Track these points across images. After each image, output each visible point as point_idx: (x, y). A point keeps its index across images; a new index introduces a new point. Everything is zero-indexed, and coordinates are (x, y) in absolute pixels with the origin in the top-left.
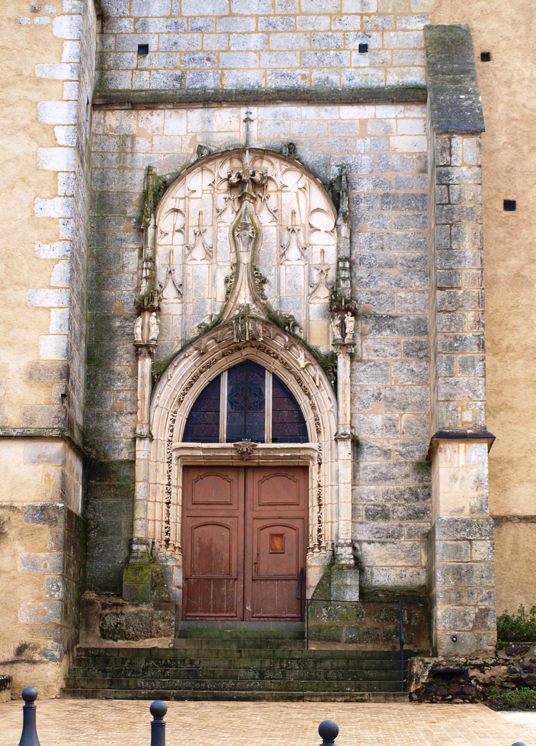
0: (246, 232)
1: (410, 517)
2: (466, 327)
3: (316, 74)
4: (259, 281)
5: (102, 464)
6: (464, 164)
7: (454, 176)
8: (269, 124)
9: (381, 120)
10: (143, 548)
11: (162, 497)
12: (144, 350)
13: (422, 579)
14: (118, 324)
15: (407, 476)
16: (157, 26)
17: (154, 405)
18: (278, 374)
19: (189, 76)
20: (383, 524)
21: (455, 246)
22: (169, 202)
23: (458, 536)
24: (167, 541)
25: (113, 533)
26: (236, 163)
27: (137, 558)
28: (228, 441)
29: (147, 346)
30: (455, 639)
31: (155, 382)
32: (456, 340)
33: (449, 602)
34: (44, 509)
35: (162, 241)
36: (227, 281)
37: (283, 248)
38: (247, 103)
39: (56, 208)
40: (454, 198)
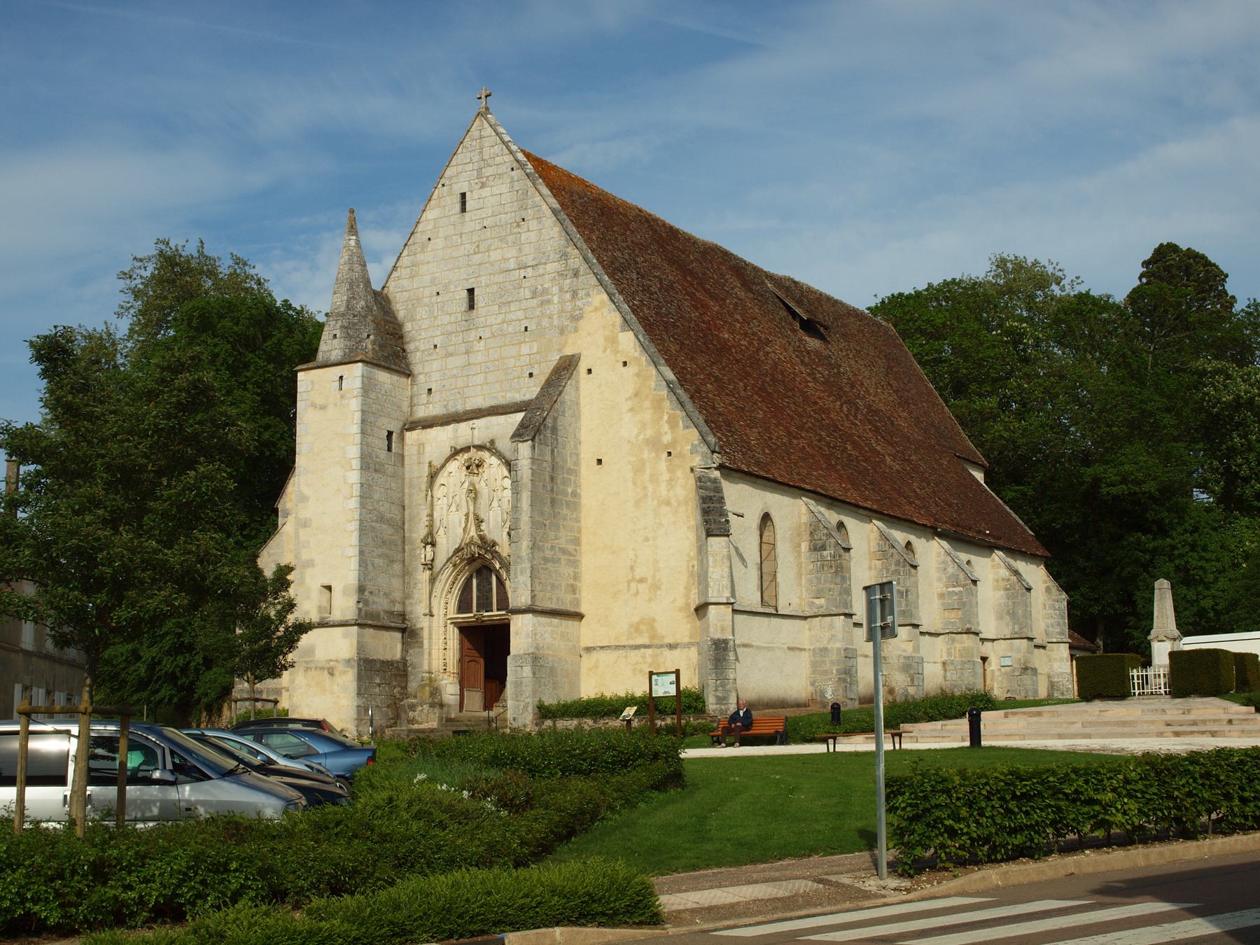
0: (473, 493)
3: (509, 395)
4: (479, 521)
16: (435, 376)
19: (450, 404)
22: (440, 479)
34: (349, 660)
39: (354, 503)
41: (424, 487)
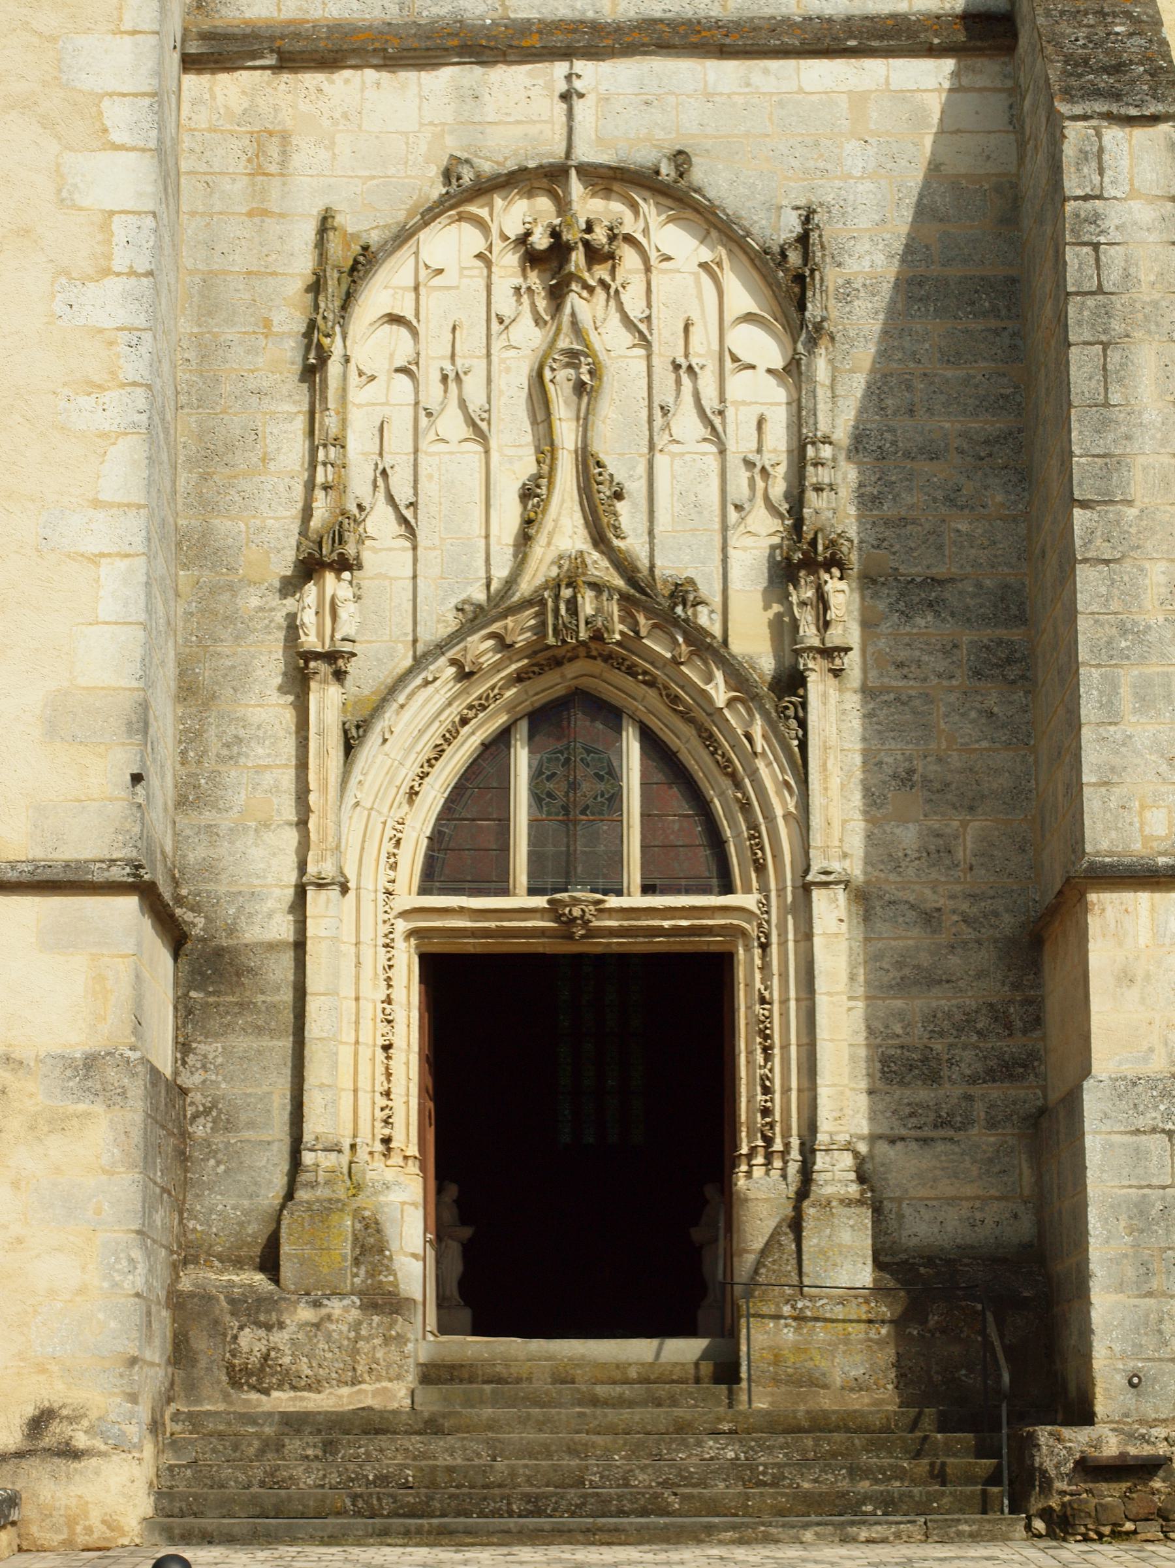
1: (991, 1076)
2: (1149, 600)
5: (219, 952)
6: (1133, 194)
7: (1111, 223)
8: (627, 107)
9: (901, 96)
10: (328, 1161)
11: (372, 1034)
12: (324, 668)
13: (1025, 1228)
14: (255, 602)
15: (980, 975)
17: (350, 801)
18: (654, 724)
20: (923, 1094)
21: (1115, 398)
23: (1141, 1122)
24: (386, 1141)
25: (251, 1125)
26: (544, 204)
27: (313, 1185)
28: (532, 892)
29: (331, 657)
30: (1134, 1383)
31: (349, 748)
32: (1124, 632)
33: (1120, 1287)
34: (91, 1063)
35: (357, 395)
36: (526, 494)
37: (658, 413)
38: (567, 53)
39: (110, 304)
40: (1112, 279)
41: (290, 320)
